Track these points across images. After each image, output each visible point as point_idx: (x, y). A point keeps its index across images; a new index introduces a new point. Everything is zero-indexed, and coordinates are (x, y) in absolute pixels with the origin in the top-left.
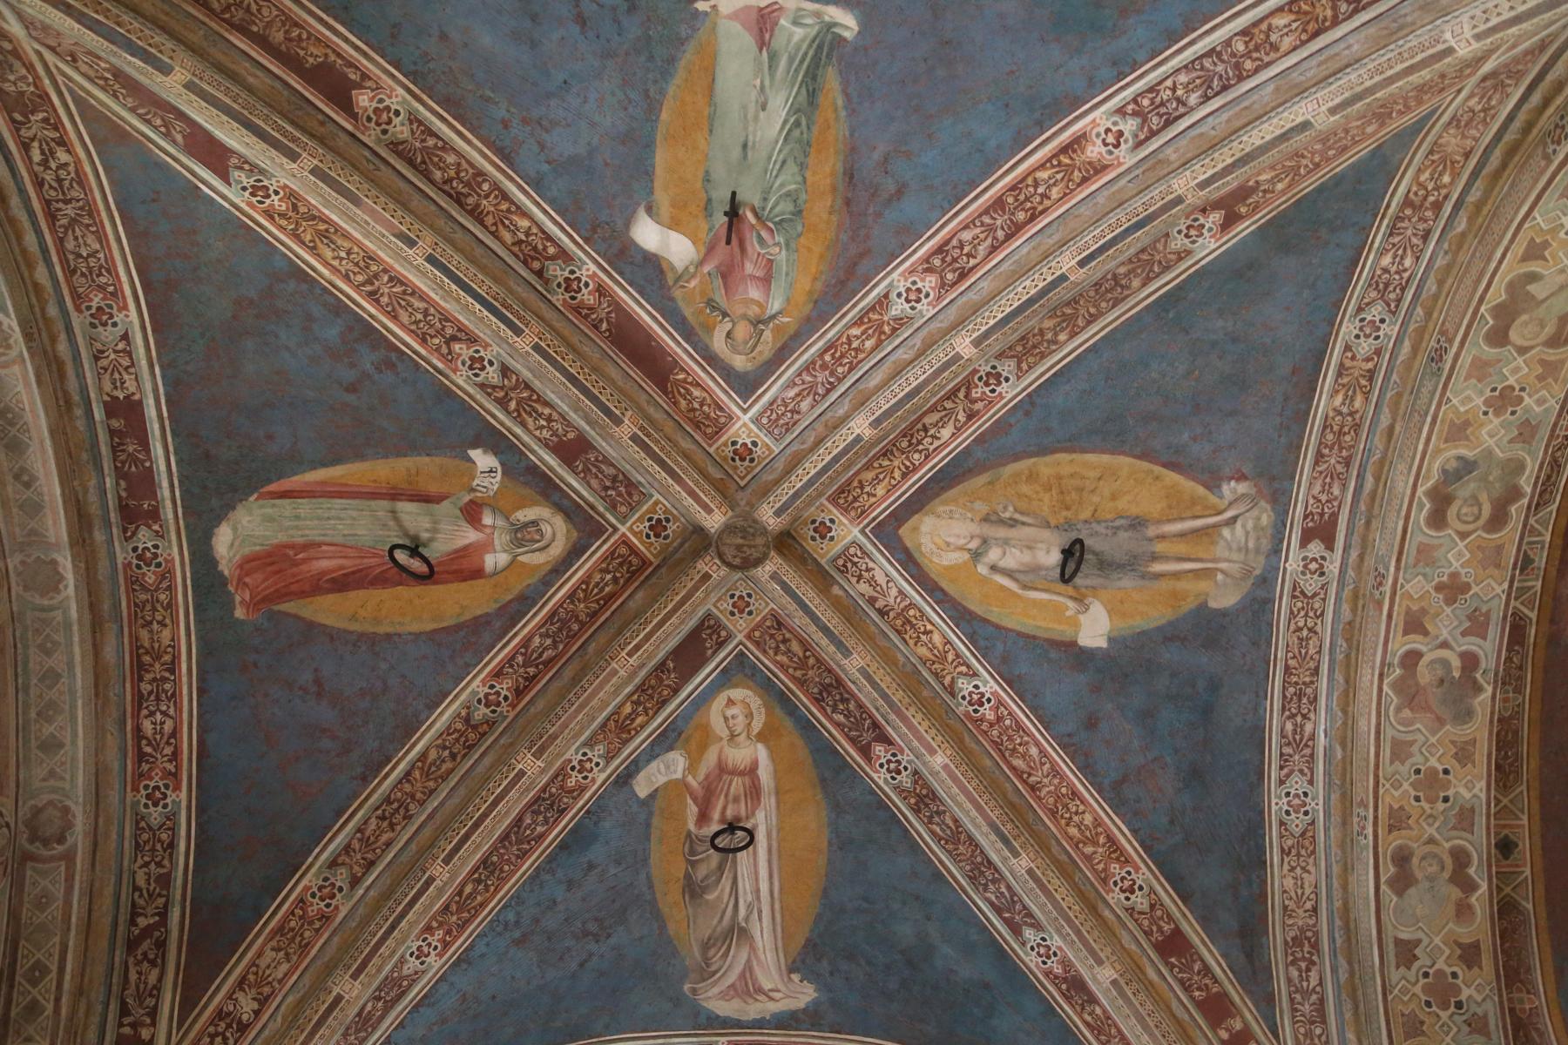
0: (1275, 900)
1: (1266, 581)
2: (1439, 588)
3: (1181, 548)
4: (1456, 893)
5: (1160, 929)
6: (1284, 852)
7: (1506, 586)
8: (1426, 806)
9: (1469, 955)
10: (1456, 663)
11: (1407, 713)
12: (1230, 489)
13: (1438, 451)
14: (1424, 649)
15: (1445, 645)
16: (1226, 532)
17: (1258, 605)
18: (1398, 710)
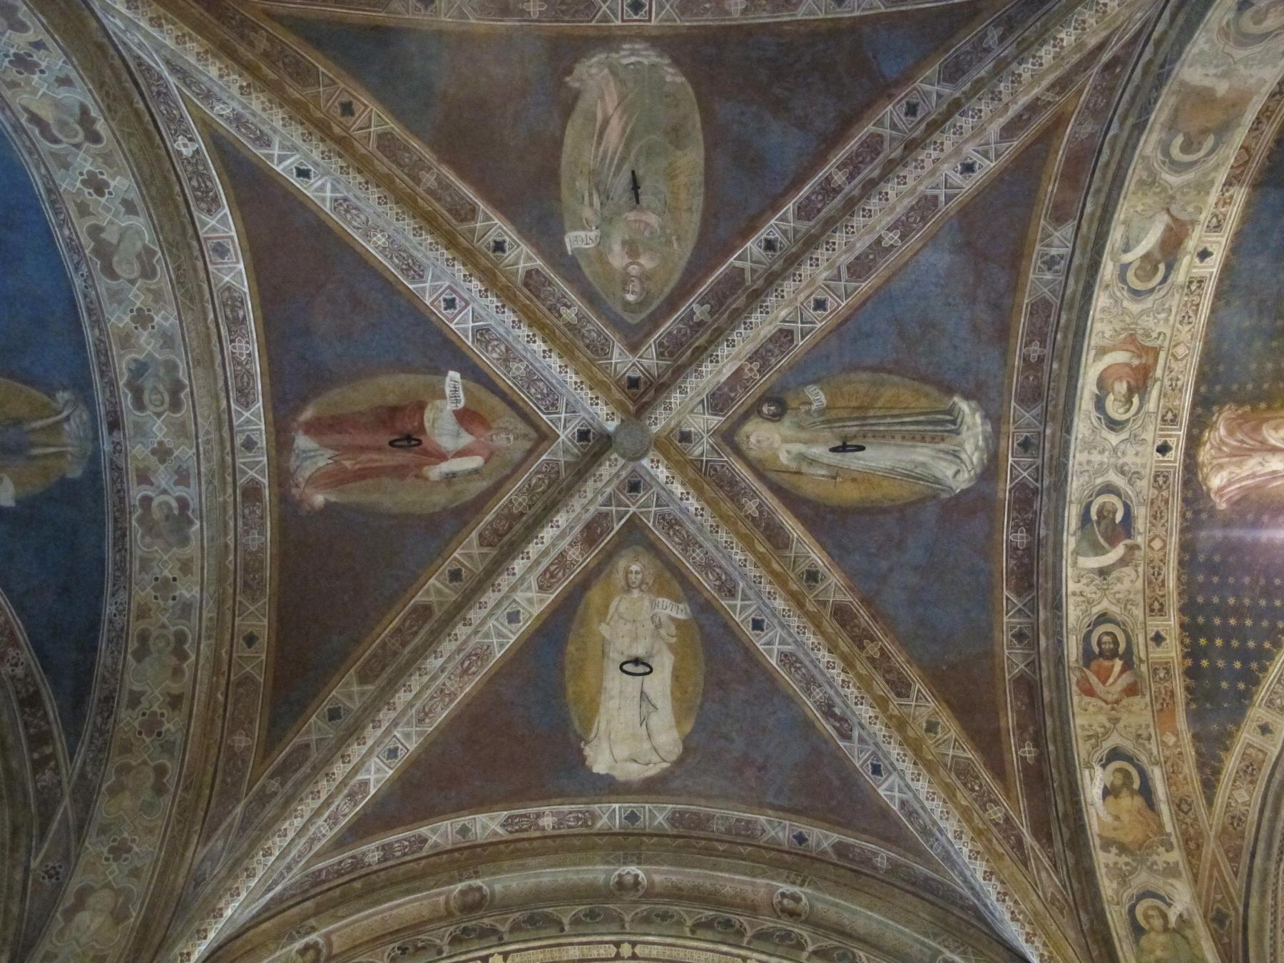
0: (99, 671)
1: (95, 458)
2: (154, 452)
3: (43, 438)
4: (173, 661)
5: (27, 690)
6: (110, 641)
7: (194, 450)
8: (162, 603)
9: (175, 702)
10: (174, 504)
11: (148, 540)
12: (63, 396)
13: (121, 356)
14: (150, 493)
15: (165, 492)
16: (66, 426)
17: (94, 474)
18: (143, 536)
